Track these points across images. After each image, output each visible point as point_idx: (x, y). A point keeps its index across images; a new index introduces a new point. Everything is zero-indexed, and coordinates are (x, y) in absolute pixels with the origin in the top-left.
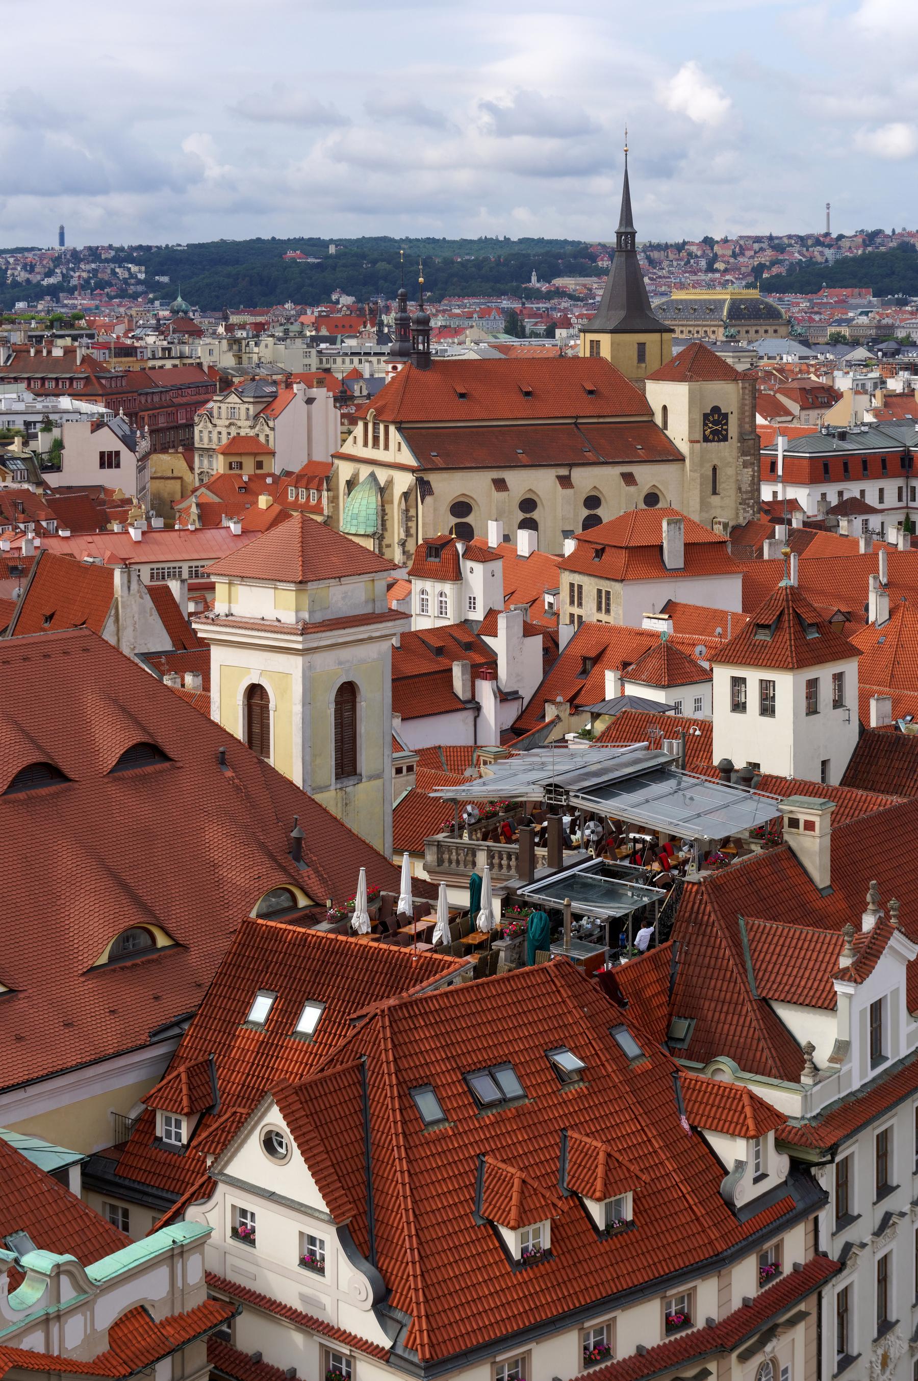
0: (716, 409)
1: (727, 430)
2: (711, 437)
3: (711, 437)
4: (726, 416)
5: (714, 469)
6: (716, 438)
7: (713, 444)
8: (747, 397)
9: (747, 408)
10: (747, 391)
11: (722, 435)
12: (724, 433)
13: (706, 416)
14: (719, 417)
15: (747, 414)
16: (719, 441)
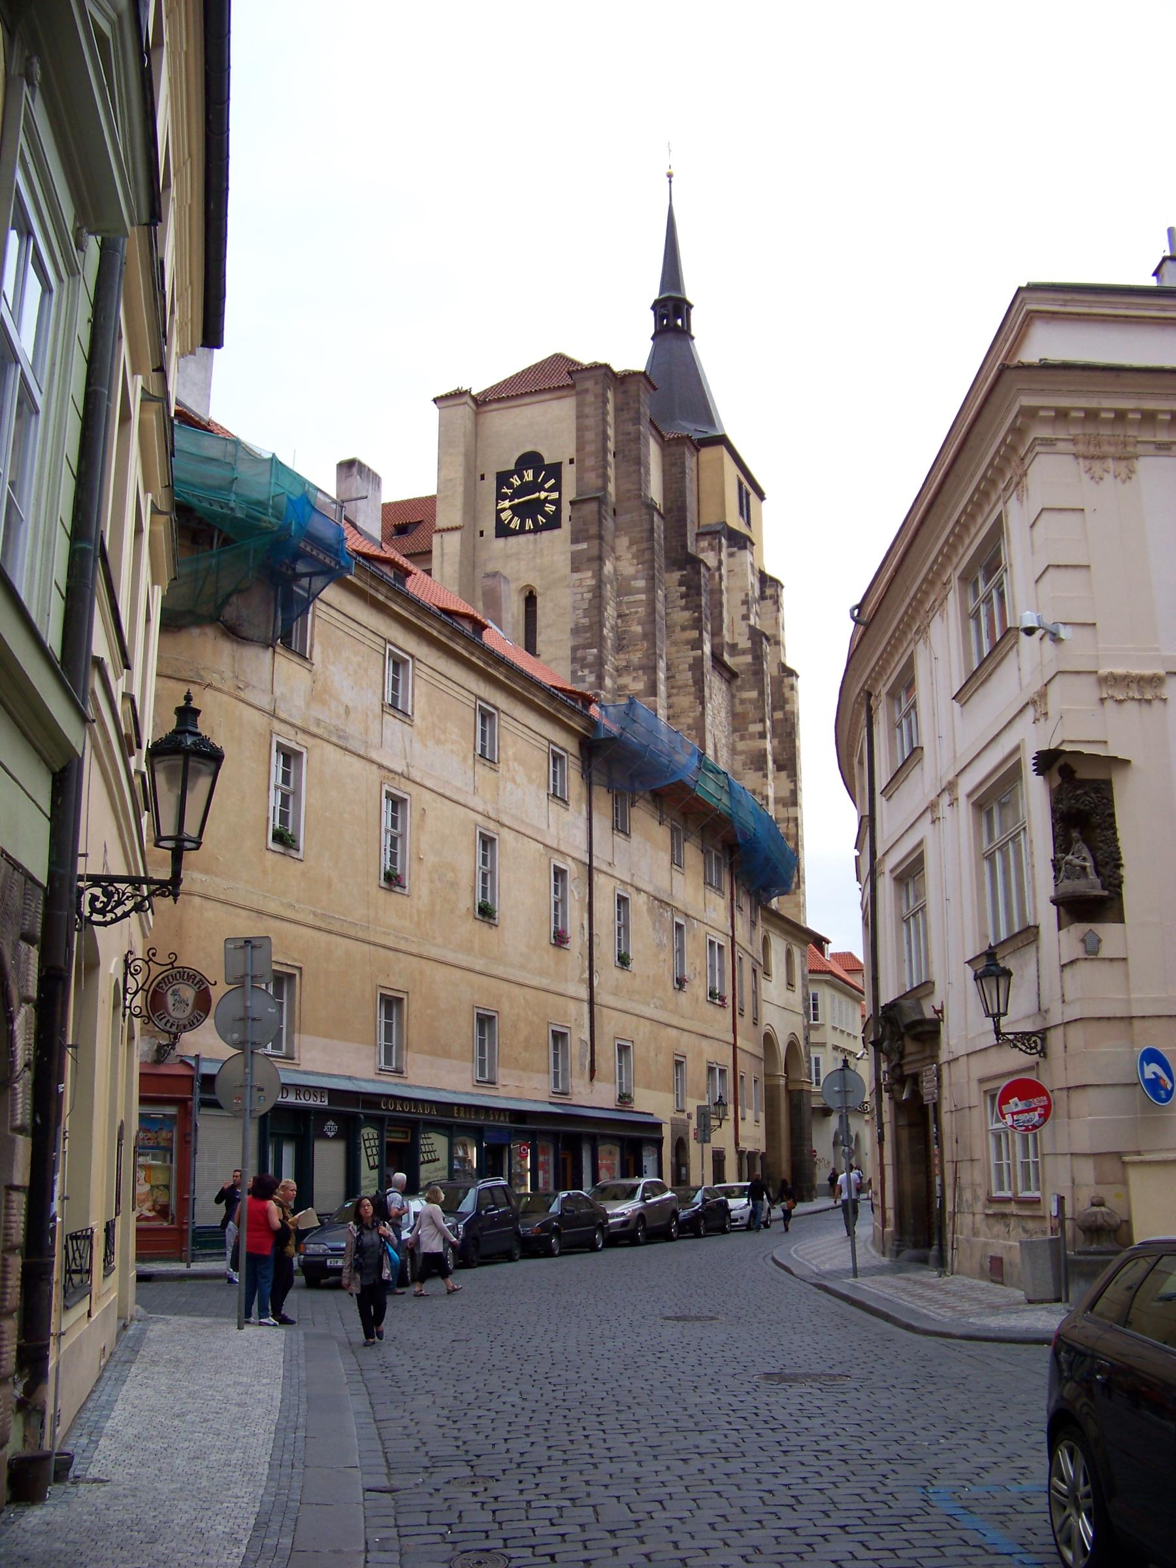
0: (530, 460)
1: (557, 503)
2: (516, 523)
3: (516, 523)
4: (555, 471)
5: (530, 600)
6: (529, 524)
7: (522, 539)
8: (588, 410)
9: (590, 435)
10: (590, 398)
11: (545, 514)
12: (550, 508)
13: (503, 478)
14: (536, 476)
15: (590, 448)
16: (537, 529)
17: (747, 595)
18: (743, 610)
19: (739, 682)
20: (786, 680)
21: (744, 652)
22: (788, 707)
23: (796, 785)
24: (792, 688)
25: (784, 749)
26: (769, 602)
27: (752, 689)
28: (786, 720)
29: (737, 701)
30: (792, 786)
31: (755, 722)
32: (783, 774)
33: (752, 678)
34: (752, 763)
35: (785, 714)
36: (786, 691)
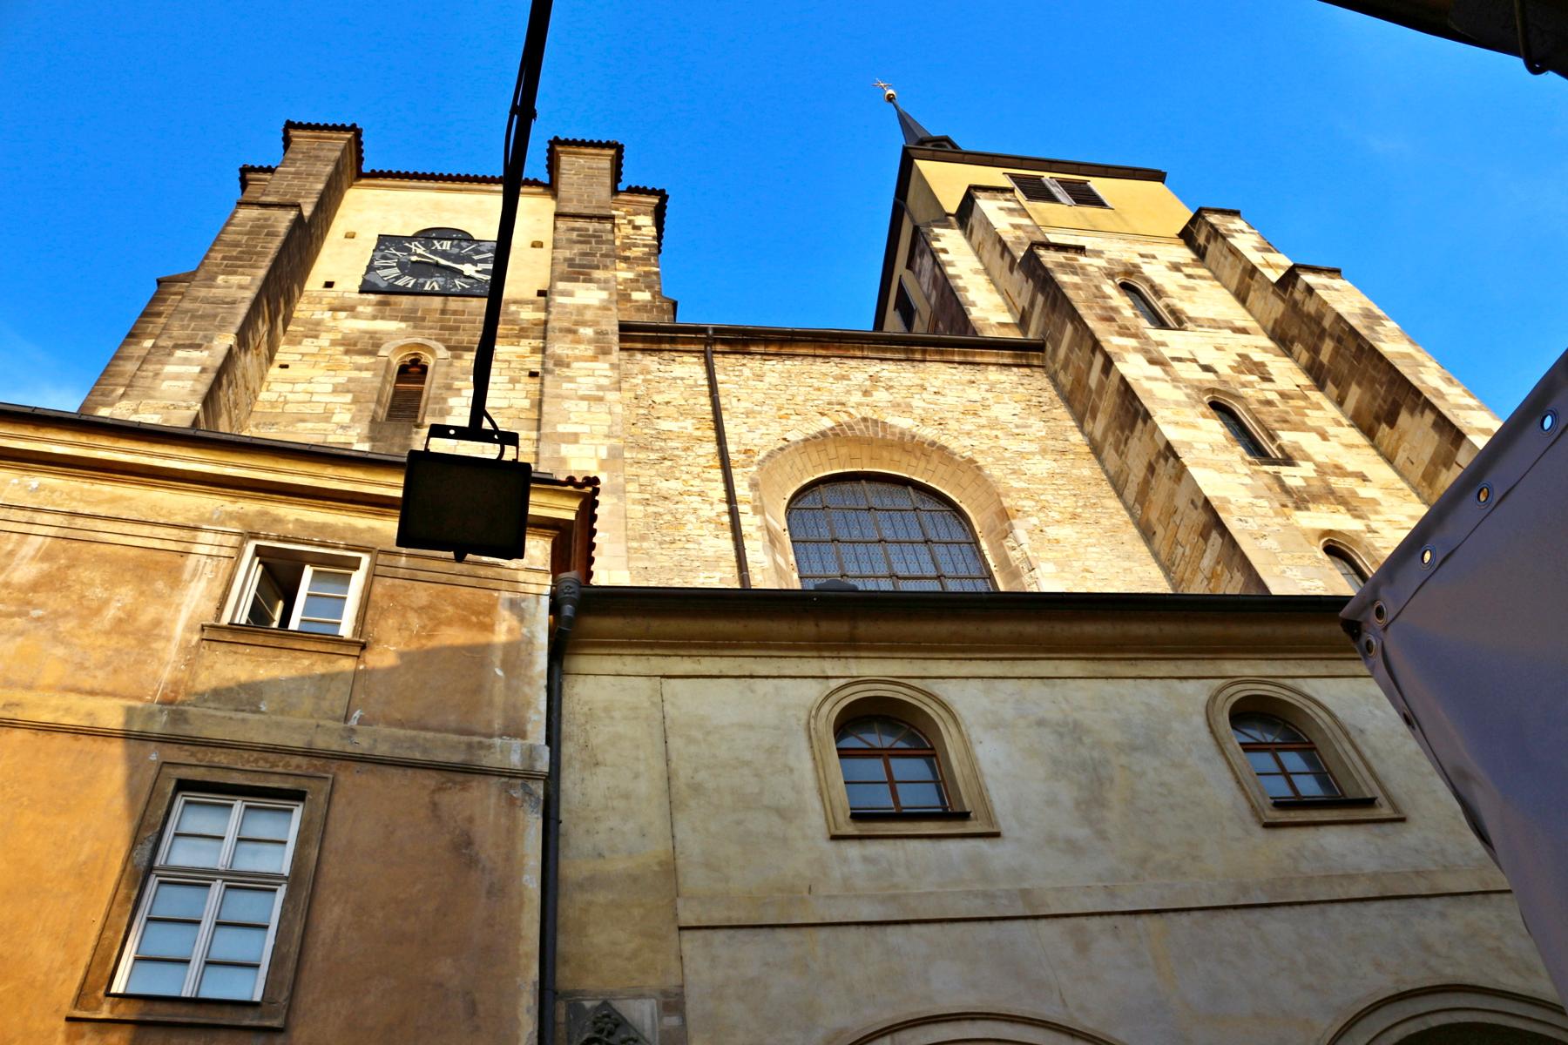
17: (1000, 240)
18: (1007, 259)
19: (1049, 347)
20: (1298, 295)
21: (1032, 304)
22: (1327, 323)
23: (1433, 408)
24: (1310, 290)
25: (1373, 381)
26: (1211, 248)
27: (1062, 332)
28: (1339, 341)
29: (1062, 376)
30: (1429, 417)
31: (1091, 364)
32: (1404, 418)
33: (1055, 318)
34: (1122, 431)
35: (1332, 336)
36: (1310, 307)
